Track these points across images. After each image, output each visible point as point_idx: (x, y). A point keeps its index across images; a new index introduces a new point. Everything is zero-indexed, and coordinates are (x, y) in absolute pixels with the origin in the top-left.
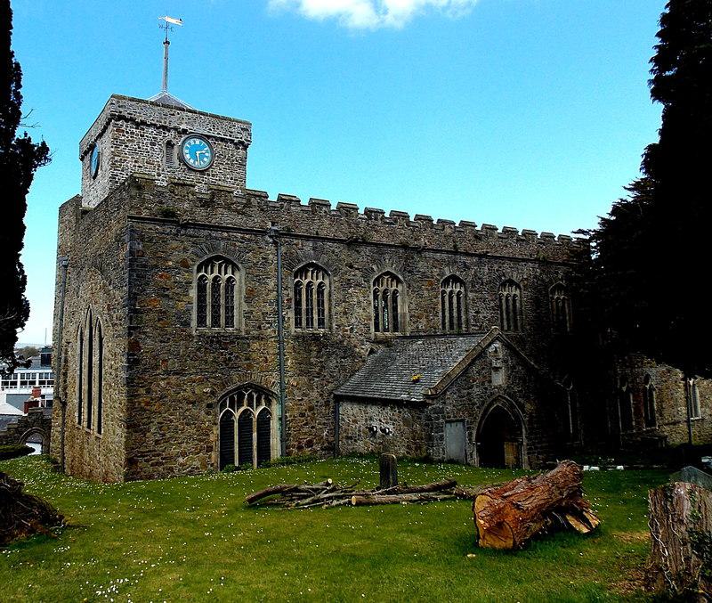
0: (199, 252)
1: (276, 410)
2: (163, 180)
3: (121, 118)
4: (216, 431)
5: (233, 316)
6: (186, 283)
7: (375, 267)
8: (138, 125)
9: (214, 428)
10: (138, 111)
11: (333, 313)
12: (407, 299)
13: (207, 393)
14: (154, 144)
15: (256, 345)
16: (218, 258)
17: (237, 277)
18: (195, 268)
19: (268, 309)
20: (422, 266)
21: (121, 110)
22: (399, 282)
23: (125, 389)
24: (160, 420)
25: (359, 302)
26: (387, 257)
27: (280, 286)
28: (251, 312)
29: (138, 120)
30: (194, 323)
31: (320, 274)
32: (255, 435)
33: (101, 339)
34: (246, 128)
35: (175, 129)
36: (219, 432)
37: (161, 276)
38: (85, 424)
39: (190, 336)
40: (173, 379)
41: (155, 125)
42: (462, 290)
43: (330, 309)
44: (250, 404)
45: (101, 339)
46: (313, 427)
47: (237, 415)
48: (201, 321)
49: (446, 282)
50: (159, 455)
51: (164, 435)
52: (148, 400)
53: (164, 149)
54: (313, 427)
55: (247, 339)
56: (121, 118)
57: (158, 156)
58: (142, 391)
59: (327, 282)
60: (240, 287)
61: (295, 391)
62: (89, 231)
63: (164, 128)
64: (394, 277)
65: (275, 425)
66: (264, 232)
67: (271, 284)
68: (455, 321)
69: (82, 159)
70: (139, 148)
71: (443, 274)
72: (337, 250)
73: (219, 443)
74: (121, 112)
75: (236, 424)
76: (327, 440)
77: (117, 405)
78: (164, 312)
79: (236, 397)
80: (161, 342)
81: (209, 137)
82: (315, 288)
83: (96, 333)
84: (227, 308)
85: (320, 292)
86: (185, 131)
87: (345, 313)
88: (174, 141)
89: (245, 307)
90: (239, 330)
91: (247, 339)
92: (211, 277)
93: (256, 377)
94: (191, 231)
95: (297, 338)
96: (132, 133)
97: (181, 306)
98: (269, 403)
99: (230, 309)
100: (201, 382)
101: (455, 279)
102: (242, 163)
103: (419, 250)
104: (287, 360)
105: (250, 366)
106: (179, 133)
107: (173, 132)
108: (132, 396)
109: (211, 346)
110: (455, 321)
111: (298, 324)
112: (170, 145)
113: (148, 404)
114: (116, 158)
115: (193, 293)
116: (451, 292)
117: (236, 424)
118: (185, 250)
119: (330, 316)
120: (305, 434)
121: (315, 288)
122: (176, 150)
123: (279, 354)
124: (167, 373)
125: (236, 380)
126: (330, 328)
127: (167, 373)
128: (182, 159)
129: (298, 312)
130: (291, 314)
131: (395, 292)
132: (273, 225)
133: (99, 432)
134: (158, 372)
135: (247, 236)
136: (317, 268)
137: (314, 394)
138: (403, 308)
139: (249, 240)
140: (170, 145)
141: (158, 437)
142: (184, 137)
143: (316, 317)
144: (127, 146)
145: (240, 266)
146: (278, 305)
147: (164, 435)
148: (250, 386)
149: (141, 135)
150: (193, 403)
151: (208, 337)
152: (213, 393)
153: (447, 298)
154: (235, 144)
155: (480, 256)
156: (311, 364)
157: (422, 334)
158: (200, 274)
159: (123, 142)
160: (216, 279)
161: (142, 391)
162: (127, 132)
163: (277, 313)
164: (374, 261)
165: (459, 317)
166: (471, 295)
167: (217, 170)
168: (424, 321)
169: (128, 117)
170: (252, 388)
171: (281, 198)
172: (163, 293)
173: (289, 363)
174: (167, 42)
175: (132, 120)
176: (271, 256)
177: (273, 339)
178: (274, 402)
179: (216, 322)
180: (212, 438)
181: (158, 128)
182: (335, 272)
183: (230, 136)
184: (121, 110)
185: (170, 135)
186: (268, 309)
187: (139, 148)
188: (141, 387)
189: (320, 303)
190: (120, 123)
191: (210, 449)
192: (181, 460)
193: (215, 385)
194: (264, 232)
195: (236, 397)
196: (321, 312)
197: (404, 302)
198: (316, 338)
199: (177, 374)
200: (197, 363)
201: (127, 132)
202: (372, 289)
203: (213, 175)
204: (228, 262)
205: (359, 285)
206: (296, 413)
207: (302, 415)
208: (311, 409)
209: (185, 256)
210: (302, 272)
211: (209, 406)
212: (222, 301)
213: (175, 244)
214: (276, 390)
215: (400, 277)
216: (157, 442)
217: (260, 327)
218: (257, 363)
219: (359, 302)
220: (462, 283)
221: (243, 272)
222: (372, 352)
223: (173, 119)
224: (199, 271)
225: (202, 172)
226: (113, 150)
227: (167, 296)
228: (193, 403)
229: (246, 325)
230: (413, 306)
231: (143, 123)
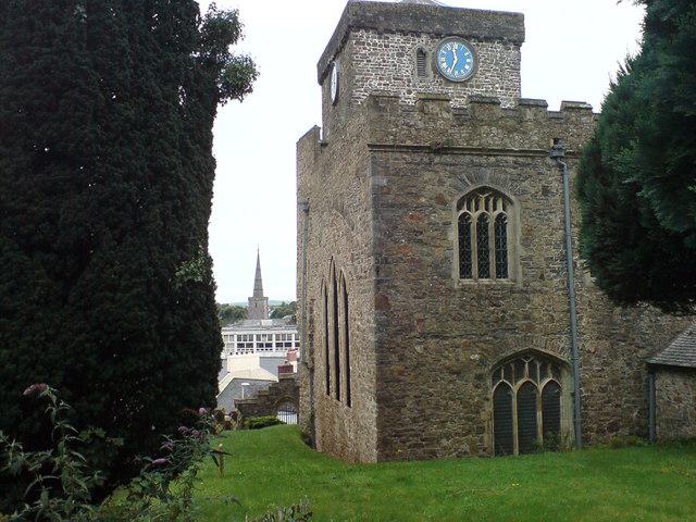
0: (459, 184)
1: (567, 384)
4: (489, 407)
5: (506, 264)
6: (444, 224)
9: (486, 403)
13: (475, 361)
14: (401, 55)
15: (537, 300)
16: (483, 190)
17: (509, 213)
18: (455, 204)
19: (554, 253)
23: (374, 355)
24: (417, 393)
27: (568, 222)
28: (530, 258)
30: (456, 273)
32: (539, 414)
33: (346, 295)
34: (516, 20)
36: (491, 409)
37: (412, 217)
38: (333, 394)
39: (450, 290)
40: (432, 343)
44: (532, 374)
45: (346, 295)
46: (617, 406)
47: (515, 388)
48: (465, 271)
50: (417, 436)
51: (423, 411)
52: (400, 368)
53: (415, 59)
54: (617, 406)
55: (526, 292)
57: (407, 67)
58: (394, 358)
60: (515, 226)
61: (593, 359)
62: (327, 167)
65: (565, 403)
67: (556, 220)
69: (321, 82)
73: (492, 423)
75: (514, 400)
76: (638, 424)
77: (366, 374)
78: (418, 262)
79: (512, 365)
80: (415, 297)
83: (340, 288)
84: (498, 253)
88: (426, 49)
89: (522, 251)
90: (515, 281)
91: (526, 292)
92: (475, 215)
93: (541, 344)
94: (448, 159)
96: (375, 44)
97: (438, 253)
98: (557, 373)
99: (502, 255)
100: (467, 347)
102: (516, 69)
104: (581, 318)
107: (424, 37)
108: (381, 363)
112: (421, 53)
113: (401, 373)
115: (453, 235)
117: (514, 400)
118: (441, 183)
120: (608, 414)
124: (424, 335)
125: (514, 344)
127: (424, 335)
128: (437, 71)
132: (556, 141)
133: (349, 404)
134: (413, 334)
135: (521, 160)
137: (620, 363)
141: (415, 414)
145: (513, 198)
146: (565, 247)
147: (423, 411)
150: (458, 373)
152: (482, 363)
154: (505, 44)
158: (461, 212)
159: (364, 56)
160: (482, 218)
161: (394, 358)
162: (369, 44)
167: (482, 78)
172: (415, 236)
177: (560, 293)
178: (565, 372)
179: (484, 272)
180: (483, 416)
186: (554, 253)
191: (481, 430)
192: (444, 442)
193: (485, 350)
195: (512, 365)
199: (437, 337)
200: (461, 325)
201: (369, 44)
203: (478, 87)
204: (497, 194)
206: (594, 387)
207: (603, 390)
208: (614, 382)
209: (440, 190)
211: (479, 377)
212: (492, 245)
213: (427, 176)
214: (564, 357)
216: (414, 420)
217: (542, 277)
218: (540, 324)
221: (518, 207)
224: (459, 208)
225: (463, 83)
227: (420, 241)
228: (458, 373)
229: (525, 275)
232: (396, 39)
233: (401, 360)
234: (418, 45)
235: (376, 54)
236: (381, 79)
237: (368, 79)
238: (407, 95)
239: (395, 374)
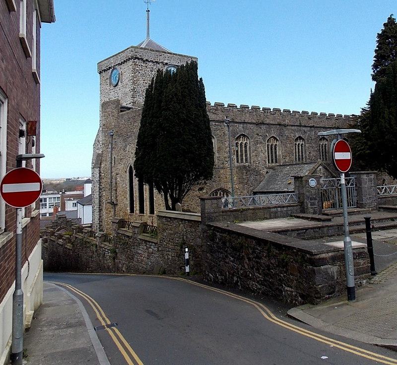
3: (136, 58)
7: (268, 135)
8: (144, 61)
11: (251, 155)
12: (281, 148)
15: (222, 171)
19: (226, 155)
20: (287, 133)
22: (277, 140)
25: (262, 151)
26: (272, 129)
29: (144, 59)
31: (245, 139)
35: (162, 63)
41: (152, 61)
42: (303, 143)
43: (250, 155)
49: (296, 140)
56: (136, 58)
59: (248, 142)
63: (157, 62)
64: (275, 138)
66: (223, 122)
68: (301, 157)
71: (296, 136)
72: (252, 128)
82: (244, 145)
85: (246, 147)
86: (166, 64)
87: (256, 156)
93: (223, 185)
95: (237, 167)
96: (142, 66)
98: (227, 196)
101: (300, 138)
103: (285, 126)
105: (220, 181)
106: (164, 65)
107: (161, 64)
110: (301, 157)
111: (238, 162)
116: (299, 144)
119: (250, 158)
121: (244, 145)
123: (231, 175)
126: (250, 163)
129: (237, 156)
130: (235, 157)
131: (276, 145)
135: (217, 123)
136: (244, 135)
138: (279, 152)
139: (218, 125)
143: (244, 158)
146: (230, 153)
148: (220, 189)
152: (207, 192)
153: (297, 146)
155: (311, 127)
156: (244, 179)
157: (287, 164)
159: (137, 70)
163: (230, 157)
164: (267, 132)
165: (302, 155)
166: (307, 145)
168: (288, 158)
169: (140, 57)
170: (221, 189)
171: (229, 106)
173: (235, 179)
174: (149, 11)
175: (142, 59)
176: (226, 132)
178: (230, 195)
181: (154, 63)
182: (252, 138)
186: (226, 155)
189: (246, 151)
190: (136, 61)
194: (223, 122)
196: (246, 156)
197: (279, 150)
198: (245, 167)
202: (267, 144)
205: (261, 143)
210: (238, 138)
214: (230, 190)
215: (278, 138)
217: (223, 164)
219: (262, 151)
220: (303, 140)
221: (216, 139)
222: (267, 172)
230: (283, 151)
231: (147, 60)
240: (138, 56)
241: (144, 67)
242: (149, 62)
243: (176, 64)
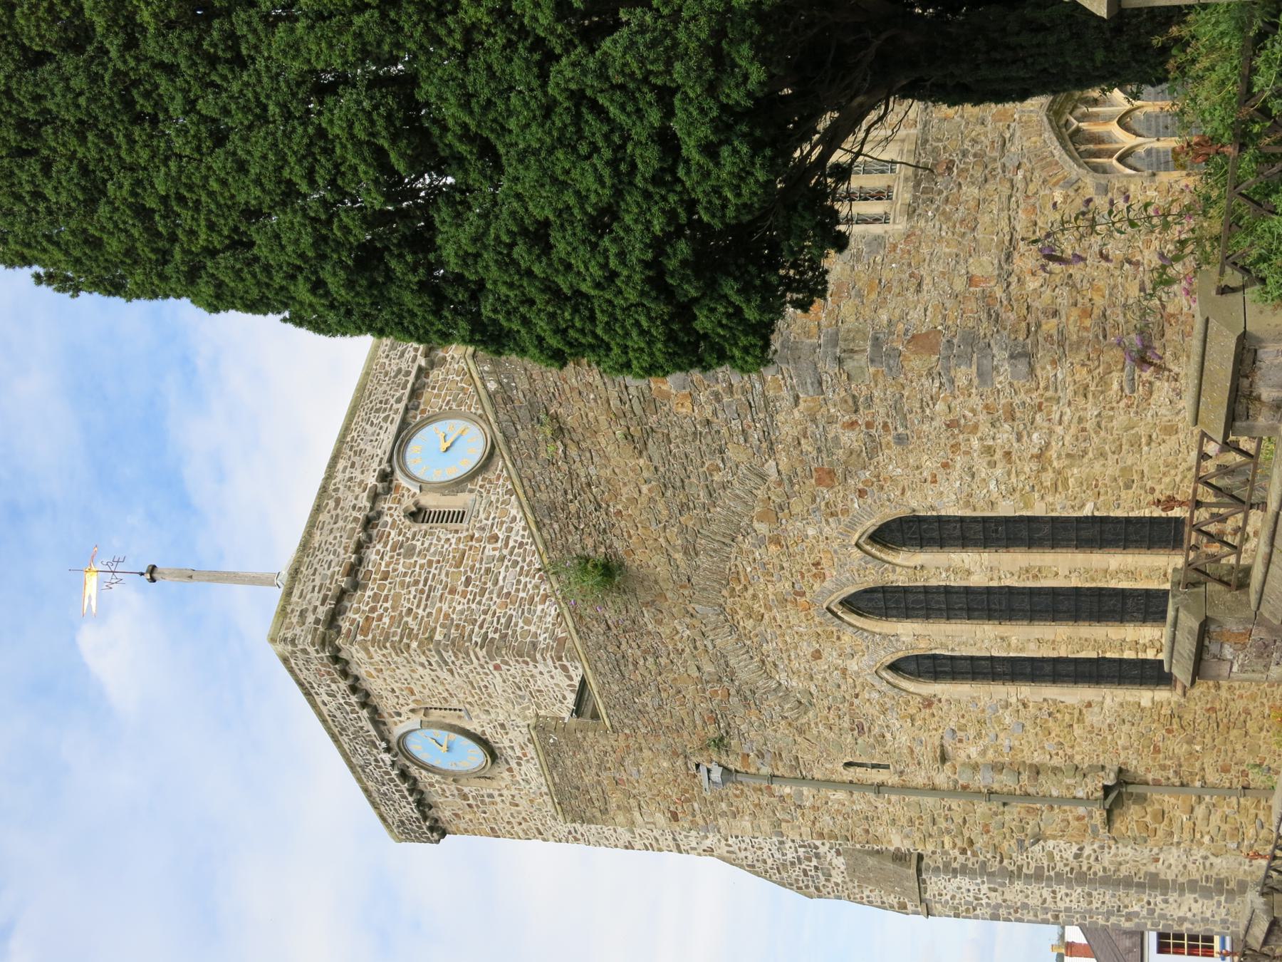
2: (510, 529)
8: (356, 586)
10: (317, 583)
14: (411, 552)
21: (311, 618)
29: (344, 582)
35: (375, 497)
39: (908, 236)
41: (360, 547)
52: (1075, 313)
53: (425, 526)
63: (369, 523)
70: (416, 583)
74: (317, 621)
79: (1082, 148)
81: (404, 424)
86: (386, 477)
88: (408, 503)
96: (375, 598)
106: (388, 490)
107: (384, 505)
109: (940, 192)
112: (417, 514)
113: (1087, 313)
114: (438, 637)
122: (431, 501)
127: (1005, 277)
128: (458, 485)
140: (417, 514)
142: (400, 478)
144: (410, 610)
149: (386, 579)
151: (915, 198)
154: (432, 365)
162: (373, 610)
169: (330, 604)
174: (153, 569)
175: (342, 595)
181: (370, 538)
183: (408, 373)
184: (311, 618)
185: (392, 511)
187: (416, 583)
188: (1039, 325)
190: (345, 626)
195: (1082, 148)
201: (373, 610)
223: (349, 500)
226: (414, 645)
231: (353, 570)
232: (373, 557)
233: (1055, 313)
234: (398, 514)
235: (397, 597)
236: (453, 591)
237: (447, 616)
238: (499, 544)
239: (1088, 323)
240: (322, 612)
241: (382, 588)
242: (360, 561)
243: (393, 429)
